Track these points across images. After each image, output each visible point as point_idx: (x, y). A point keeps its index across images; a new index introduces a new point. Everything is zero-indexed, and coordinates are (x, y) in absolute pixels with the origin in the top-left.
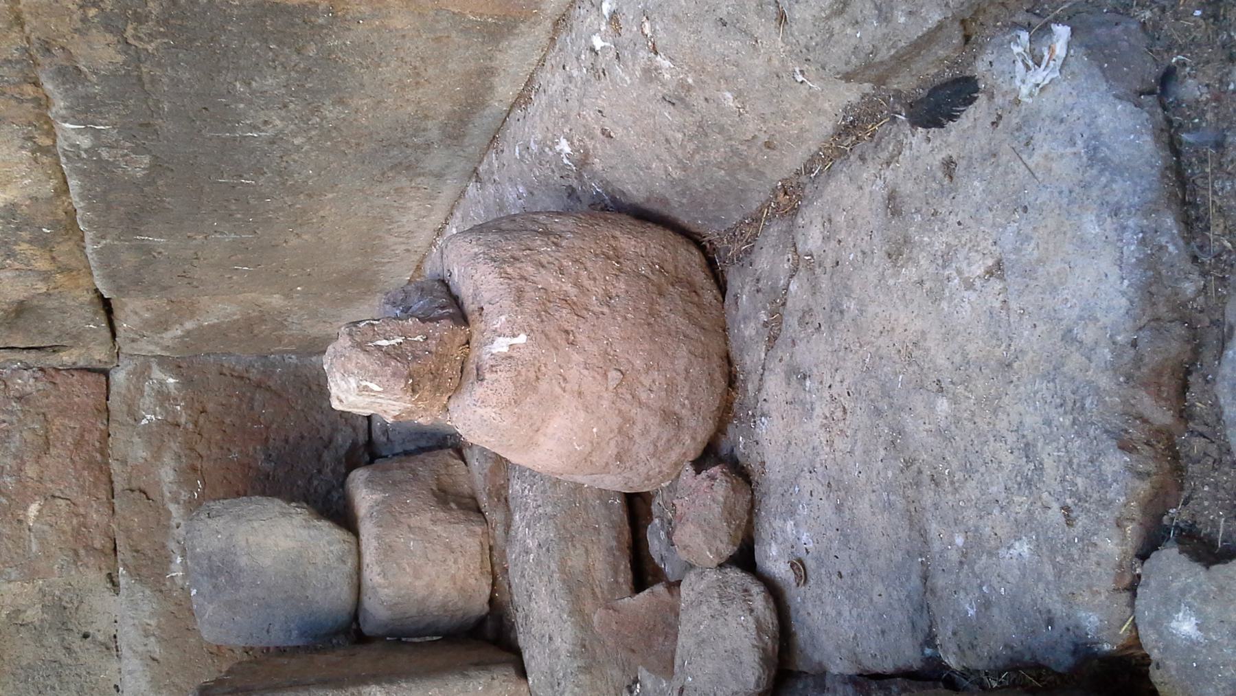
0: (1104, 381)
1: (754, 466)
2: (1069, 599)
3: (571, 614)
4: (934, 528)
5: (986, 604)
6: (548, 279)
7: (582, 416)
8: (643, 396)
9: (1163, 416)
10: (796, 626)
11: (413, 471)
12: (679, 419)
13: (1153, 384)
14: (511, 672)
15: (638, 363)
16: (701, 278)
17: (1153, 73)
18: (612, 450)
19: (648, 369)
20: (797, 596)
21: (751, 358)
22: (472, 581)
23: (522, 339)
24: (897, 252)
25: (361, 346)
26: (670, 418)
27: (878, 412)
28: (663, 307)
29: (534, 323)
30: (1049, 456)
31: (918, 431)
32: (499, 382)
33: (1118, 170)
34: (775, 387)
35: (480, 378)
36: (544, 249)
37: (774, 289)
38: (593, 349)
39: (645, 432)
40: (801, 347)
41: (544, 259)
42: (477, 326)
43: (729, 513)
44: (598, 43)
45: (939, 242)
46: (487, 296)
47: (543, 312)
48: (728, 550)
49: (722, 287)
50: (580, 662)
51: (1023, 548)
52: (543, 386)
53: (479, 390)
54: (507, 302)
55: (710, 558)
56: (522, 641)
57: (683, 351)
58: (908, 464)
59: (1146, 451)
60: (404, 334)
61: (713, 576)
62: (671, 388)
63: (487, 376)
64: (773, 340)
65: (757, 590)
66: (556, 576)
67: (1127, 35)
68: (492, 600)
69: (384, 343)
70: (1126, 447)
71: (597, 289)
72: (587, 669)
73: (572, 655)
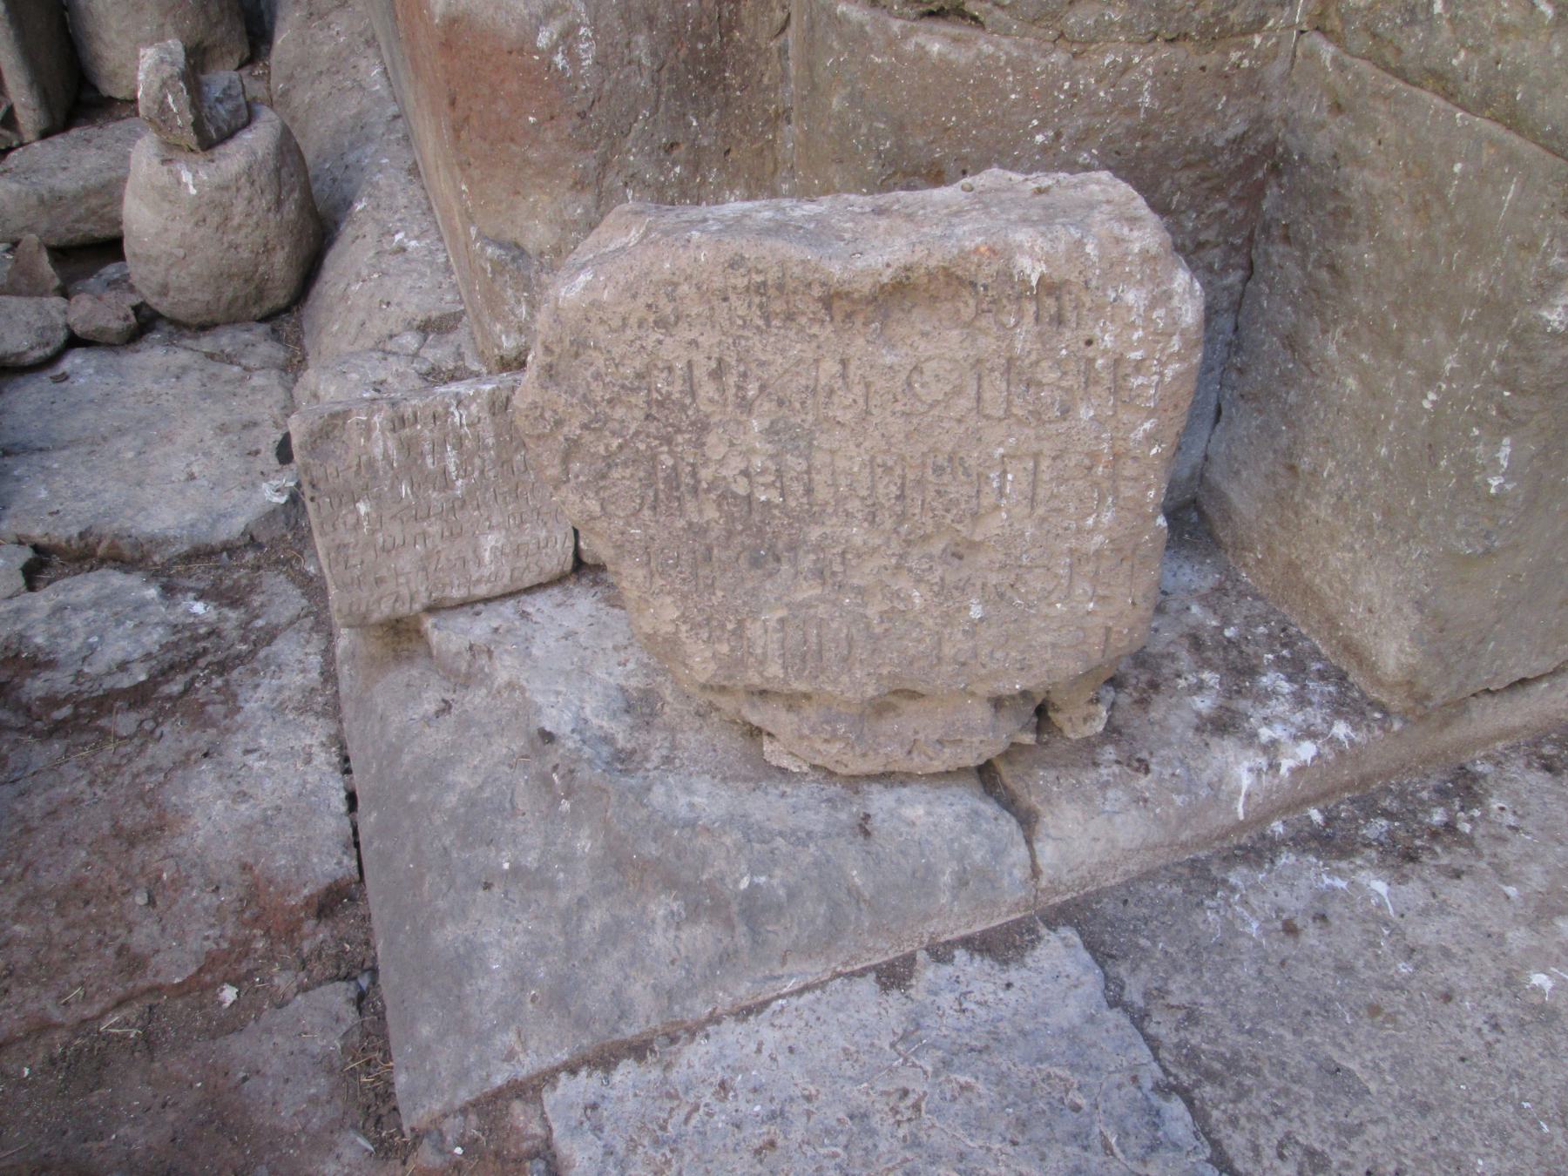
0: (116, 525)
1: (139, 346)
2: (15, 516)
3: (84, 188)
4: (66, 453)
5: (18, 479)
6: (240, 207)
7: (152, 231)
8: (173, 272)
9: (100, 551)
10: (28, 376)
11: (219, 22)
12: (166, 295)
13: (113, 546)
14: (44, 126)
15: (193, 268)
16: (268, 305)
17: (263, 539)
18: (138, 250)
19: (191, 275)
20: (46, 377)
21: (207, 343)
22: (125, 82)
23: (193, 191)
24: (223, 429)
25: (164, 84)
26: (164, 290)
27: (139, 421)
28: (237, 283)
29: (206, 199)
30: (88, 503)
31: (119, 444)
32: (164, 178)
33: (213, 526)
34: (183, 357)
35: (165, 162)
36: (263, 203)
37: (242, 356)
38: (196, 238)
39: (153, 273)
40: (197, 374)
41: (256, 202)
42: (200, 157)
43: (103, 331)
44: (398, 237)
45: (217, 451)
46: (223, 164)
47: (214, 205)
48: (78, 330)
49: (264, 319)
50: (47, 196)
51: (43, 494)
52: (166, 206)
53: (156, 161)
54: (217, 180)
55: (71, 320)
56: (74, 132)
57: (208, 297)
58: (105, 439)
59: (82, 544)
60: (180, 113)
61: (60, 321)
62: (182, 290)
63: (165, 168)
64: (211, 356)
65: (48, 351)
66: (114, 174)
67: (278, 528)
68: (111, 101)
69: (170, 99)
70: (82, 535)
71: (239, 238)
72: (42, 201)
73: (51, 190)
